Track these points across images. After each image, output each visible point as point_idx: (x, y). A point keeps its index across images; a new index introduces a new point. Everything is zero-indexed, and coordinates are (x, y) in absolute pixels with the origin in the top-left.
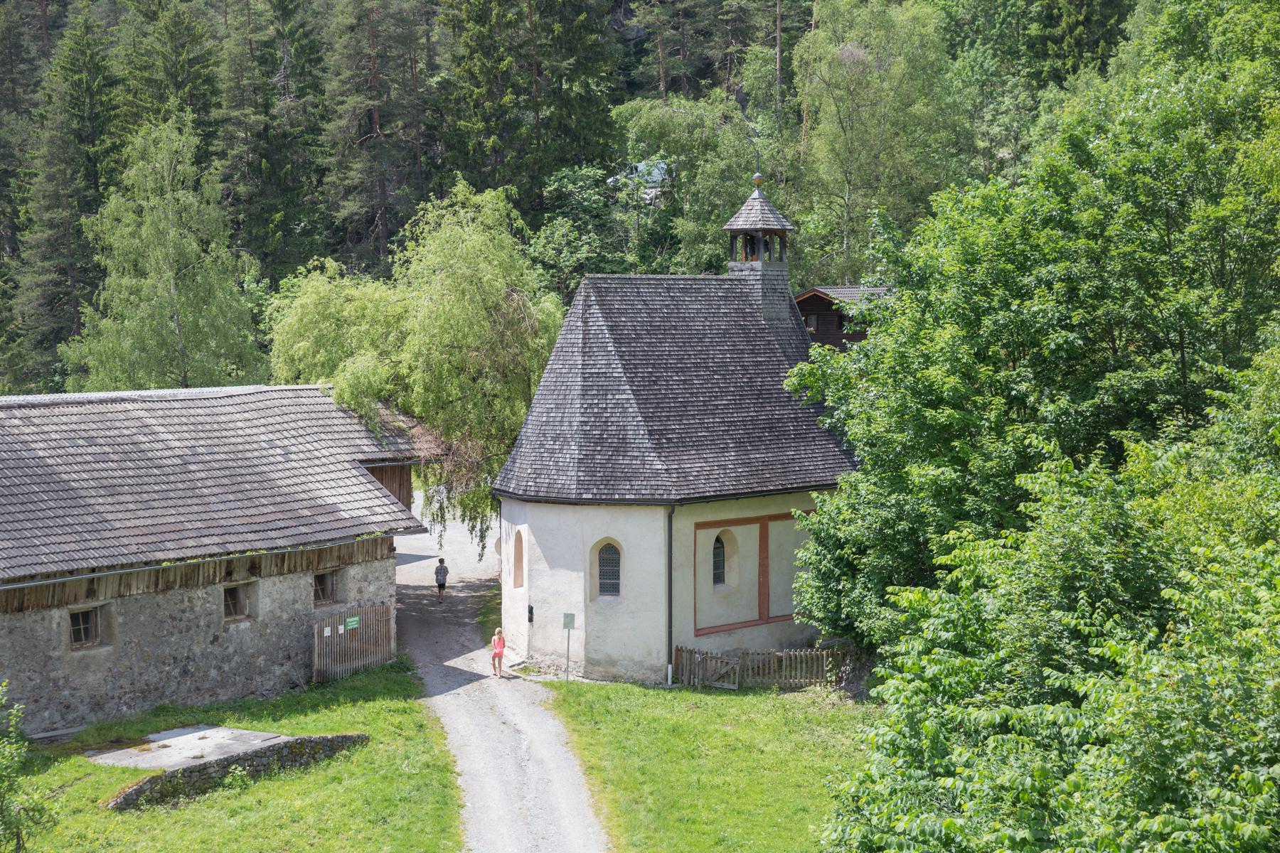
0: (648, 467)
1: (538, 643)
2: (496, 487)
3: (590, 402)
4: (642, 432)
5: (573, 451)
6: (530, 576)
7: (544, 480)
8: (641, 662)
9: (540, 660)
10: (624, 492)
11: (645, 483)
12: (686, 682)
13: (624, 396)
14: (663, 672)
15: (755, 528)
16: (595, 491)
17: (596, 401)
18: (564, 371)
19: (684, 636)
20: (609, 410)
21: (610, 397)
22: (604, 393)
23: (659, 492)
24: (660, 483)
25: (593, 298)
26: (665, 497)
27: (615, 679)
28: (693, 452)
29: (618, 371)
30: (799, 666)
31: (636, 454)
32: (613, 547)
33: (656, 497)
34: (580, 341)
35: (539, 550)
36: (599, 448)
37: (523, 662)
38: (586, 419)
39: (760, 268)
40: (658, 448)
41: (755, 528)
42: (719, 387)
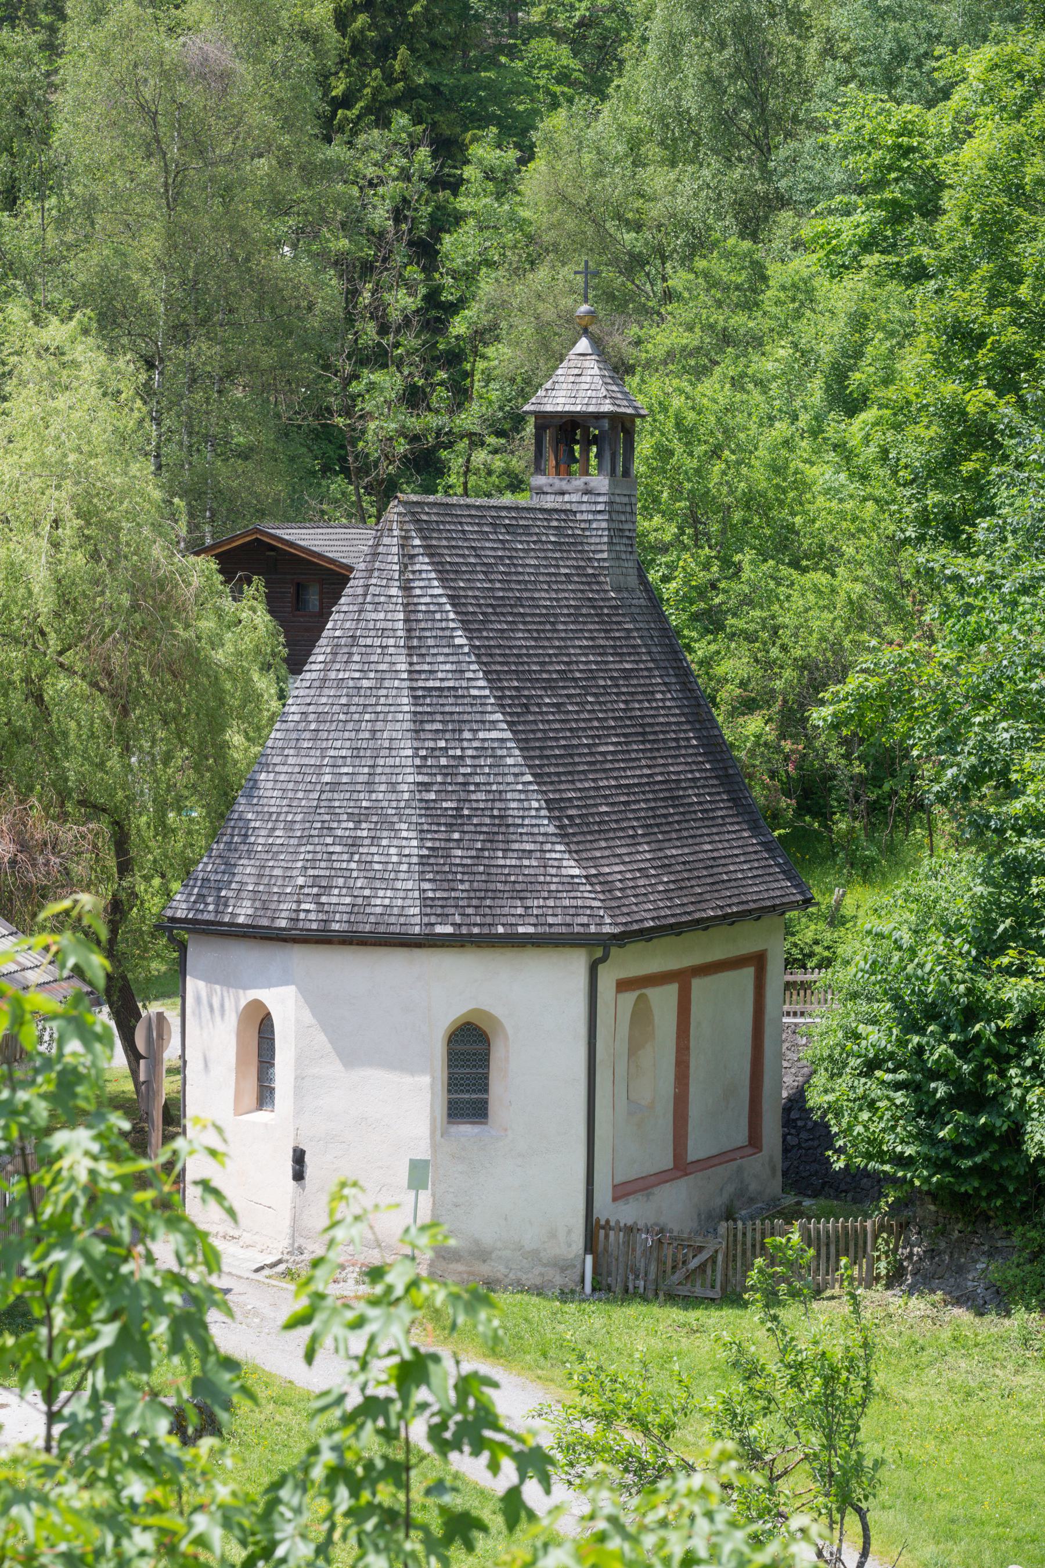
0: (553, 871)
2: (179, 914)
3: (431, 744)
4: (535, 804)
7: (338, 899)
8: (535, 1253)
10: (513, 920)
11: (551, 903)
12: (618, 1289)
13: (494, 735)
15: (672, 991)
16: (458, 919)
17: (442, 744)
18: (365, 683)
20: (469, 762)
21: (467, 735)
22: (455, 727)
24: (580, 903)
25: (417, 542)
26: (593, 929)
28: (603, 844)
29: (480, 687)
34: (400, 625)
35: (322, 1038)
36: (456, 836)
39: (605, 489)
40: (563, 836)
41: (672, 991)
42: (598, 719)
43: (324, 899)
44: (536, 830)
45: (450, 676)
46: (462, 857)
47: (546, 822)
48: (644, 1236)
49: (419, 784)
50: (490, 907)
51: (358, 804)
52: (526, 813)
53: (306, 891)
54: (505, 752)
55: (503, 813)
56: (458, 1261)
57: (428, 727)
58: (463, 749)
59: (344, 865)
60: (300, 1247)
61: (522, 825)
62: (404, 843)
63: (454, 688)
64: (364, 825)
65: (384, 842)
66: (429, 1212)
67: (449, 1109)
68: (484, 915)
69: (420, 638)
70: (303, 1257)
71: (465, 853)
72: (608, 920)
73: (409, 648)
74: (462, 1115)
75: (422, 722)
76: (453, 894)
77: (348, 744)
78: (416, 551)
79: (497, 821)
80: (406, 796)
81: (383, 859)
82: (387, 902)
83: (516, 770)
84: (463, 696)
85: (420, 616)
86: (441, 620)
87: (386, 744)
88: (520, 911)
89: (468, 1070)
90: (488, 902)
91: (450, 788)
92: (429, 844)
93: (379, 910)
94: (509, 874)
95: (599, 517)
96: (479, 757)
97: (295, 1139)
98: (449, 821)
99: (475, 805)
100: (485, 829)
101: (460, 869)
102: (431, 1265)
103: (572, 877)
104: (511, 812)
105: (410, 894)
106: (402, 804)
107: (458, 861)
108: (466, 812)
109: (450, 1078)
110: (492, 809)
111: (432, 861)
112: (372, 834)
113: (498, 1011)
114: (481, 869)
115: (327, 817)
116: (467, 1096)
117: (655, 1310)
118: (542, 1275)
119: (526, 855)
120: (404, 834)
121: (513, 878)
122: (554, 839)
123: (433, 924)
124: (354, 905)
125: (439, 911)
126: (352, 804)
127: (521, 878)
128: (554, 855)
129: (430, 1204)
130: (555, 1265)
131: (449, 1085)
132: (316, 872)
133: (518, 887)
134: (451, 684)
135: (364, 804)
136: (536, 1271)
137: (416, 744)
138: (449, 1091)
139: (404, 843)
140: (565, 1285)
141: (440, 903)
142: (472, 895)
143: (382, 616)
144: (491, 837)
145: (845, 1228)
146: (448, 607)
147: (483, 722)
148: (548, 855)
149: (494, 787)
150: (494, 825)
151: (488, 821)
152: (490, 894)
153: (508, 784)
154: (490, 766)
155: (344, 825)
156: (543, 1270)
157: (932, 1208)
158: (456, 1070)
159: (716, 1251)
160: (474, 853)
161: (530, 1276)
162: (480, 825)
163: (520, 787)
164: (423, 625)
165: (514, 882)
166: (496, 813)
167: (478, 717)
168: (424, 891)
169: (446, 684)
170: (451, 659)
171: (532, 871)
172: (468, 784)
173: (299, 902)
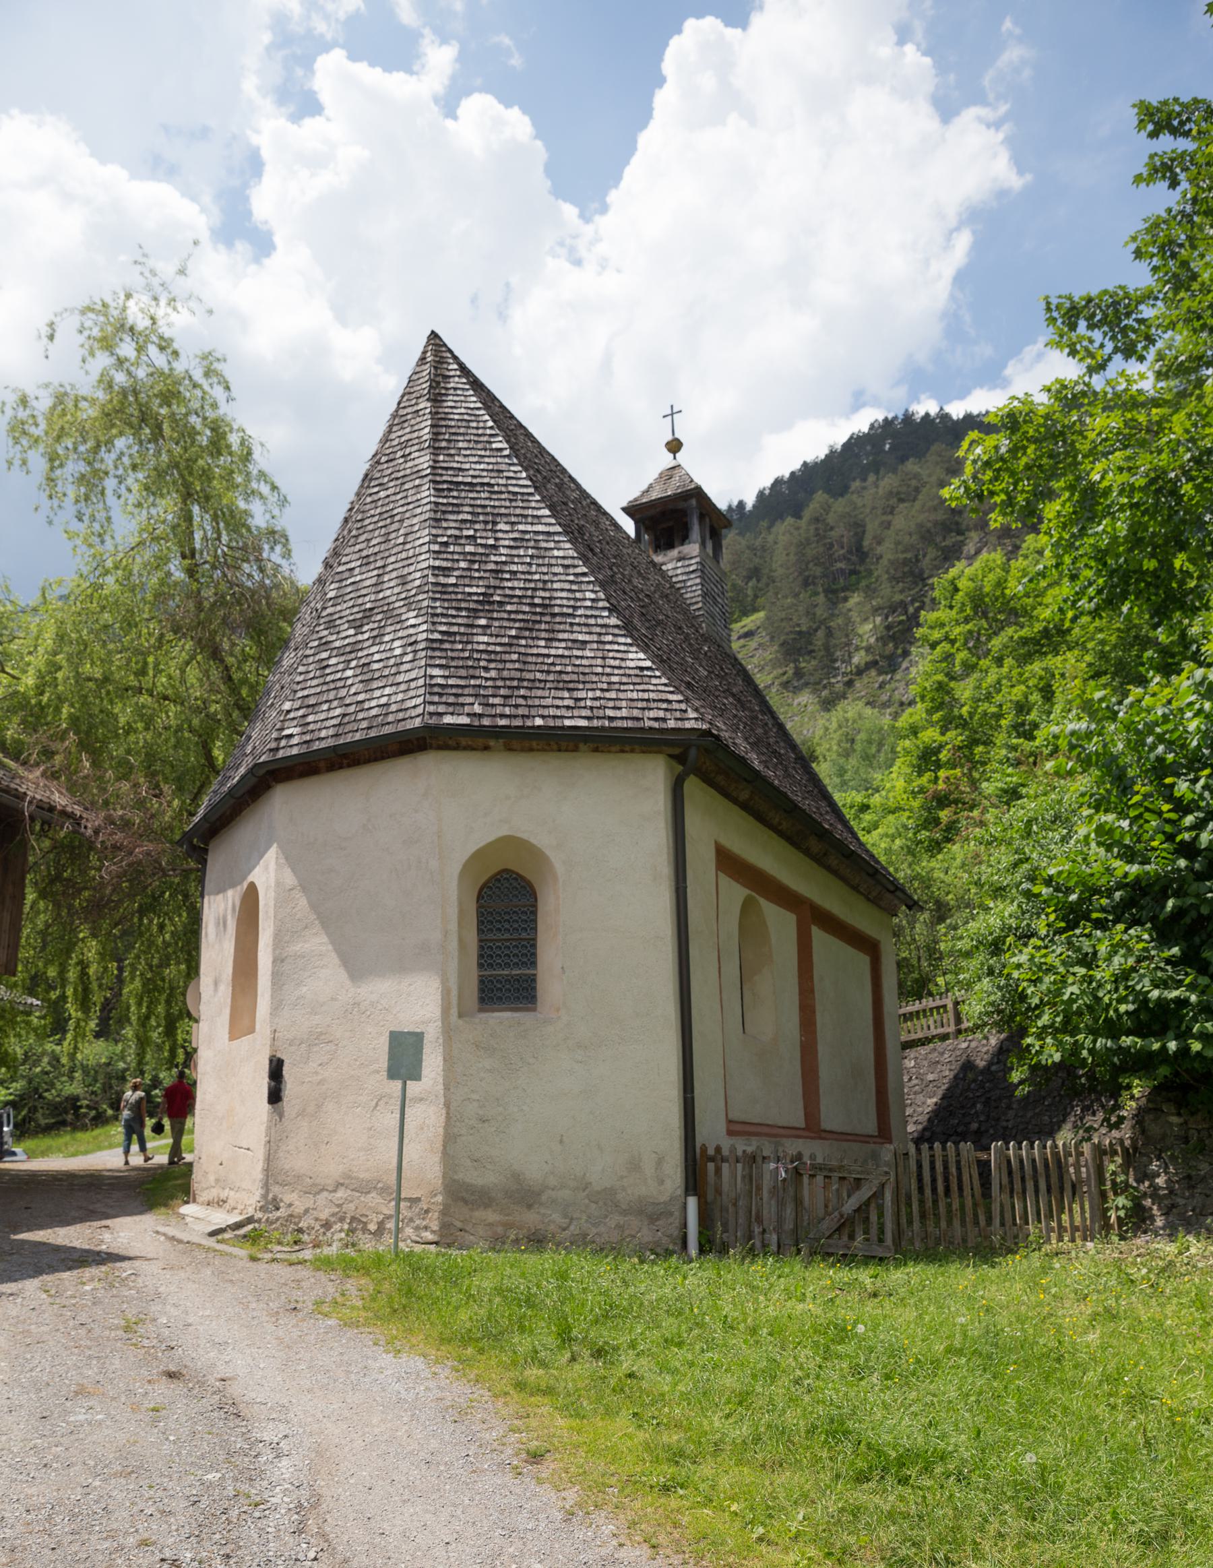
1: (296, 1161)
5: (417, 625)
6: (276, 976)
8: (610, 1192)
9: (299, 1208)
11: (613, 695)
16: (477, 709)
20: (503, 551)
23: (652, 714)
24: (652, 696)
26: (671, 724)
27: (537, 1241)
30: (1030, 1185)
31: (581, 637)
32: (519, 877)
33: (648, 724)
35: (303, 902)
37: (250, 1220)
38: (444, 564)
43: (310, 718)
44: (592, 621)
45: (485, 474)
46: (488, 644)
47: (606, 614)
48: (772, 1166)
49: (434, 568)
50: (524, 697)
51: (363, 608)
52: (579, 604)
53: (292, 715)
54: (552, 545)
55: (547, 602)
56: (487, 1206)
58: (496, 539)
59: (339, 675)
60: (274, 1199)
61: (574, 616)
62: (412, 631)
63: (488, 484)
64: (365, 628)
65: (387, 638)
66: (441, 1131)
67: (481, 990)
68: (516, 706)
69: (449, 441)
70: (278, 1214)
71: (493, 640)
73: (435, 448)
75: (444, 512)
76: (472, 682)
77: (357, 556)
78: (452, 373)
79: (538, 610)
80: (417, 583)
81: (383, 656)
82: (384, 700)
83: (566, 562)
84: (501, 493)
85: (453, 423)
86: (477, 428)
87: (401, 540)
88: (571, 703)
89: (507, 936)
90: (522, 692)
91: (477, 575)
92: (444, 628)
93: (374, 712)
94: (553, 664)
95: (692, 576)
97: (272, 1045)
98: (472, 605)
99: (508, 592)
100: (520, 617)
101: (484, 656)
102: (445, 1212)
103: (642, 669)
104: (558, 602)
105: (413, 685)
106: (413, 592)
107: (482, 647)
108: (497, 598)
109: (481, 948)
110: (532, 597)
112: (375, 633)
113: (541, 840)
114: (515, 657)
115: (326, 633)
116: (505, 972)
118: (619, 1227)
119: (578, 645)
120: (412, 622)
121: (558, 668)
122: (616, 631)
123: (441, 714)
124: (344, 715)
125: (451, 700)
126: (356, 609)
127: (569, 669)
128: (616, 647)
129: (442, 1119)
130: (640, 1212)
131: (481, 956)
132: (306, 693)
133: (566, 677)
134: (486, 480)
135: (368, 606)
136: (612, 1222)
137: (434, 531)
138: (480, 966)
139: (412, 631)
141: (454, 691)
142: (500, 683)
143: (408, 430)
144: (530, 625)
146: (487, 417)
147: (526, 516)
148: (608, 647)
149: (537, 577)
150: (535, 613)
151: (527, 609)
152: (525, 684)
153: (555, 574)
154: (532, 557)
155: (343, 634)
156: (621, 1220)
158: (490, 936)
159: (883, 1185)
160: (506, 640)
161: (602, 1229)
162: (517, 612)
163: (571, 578)
164: (453, 430)
165: (560, 672)
166: (537, 601)
167: (518, 511)
168: (432, 677)
169: (479, 480)
170: (487, 460)
171: (585, 662)
172: (503, 572)
173: (282, 729)
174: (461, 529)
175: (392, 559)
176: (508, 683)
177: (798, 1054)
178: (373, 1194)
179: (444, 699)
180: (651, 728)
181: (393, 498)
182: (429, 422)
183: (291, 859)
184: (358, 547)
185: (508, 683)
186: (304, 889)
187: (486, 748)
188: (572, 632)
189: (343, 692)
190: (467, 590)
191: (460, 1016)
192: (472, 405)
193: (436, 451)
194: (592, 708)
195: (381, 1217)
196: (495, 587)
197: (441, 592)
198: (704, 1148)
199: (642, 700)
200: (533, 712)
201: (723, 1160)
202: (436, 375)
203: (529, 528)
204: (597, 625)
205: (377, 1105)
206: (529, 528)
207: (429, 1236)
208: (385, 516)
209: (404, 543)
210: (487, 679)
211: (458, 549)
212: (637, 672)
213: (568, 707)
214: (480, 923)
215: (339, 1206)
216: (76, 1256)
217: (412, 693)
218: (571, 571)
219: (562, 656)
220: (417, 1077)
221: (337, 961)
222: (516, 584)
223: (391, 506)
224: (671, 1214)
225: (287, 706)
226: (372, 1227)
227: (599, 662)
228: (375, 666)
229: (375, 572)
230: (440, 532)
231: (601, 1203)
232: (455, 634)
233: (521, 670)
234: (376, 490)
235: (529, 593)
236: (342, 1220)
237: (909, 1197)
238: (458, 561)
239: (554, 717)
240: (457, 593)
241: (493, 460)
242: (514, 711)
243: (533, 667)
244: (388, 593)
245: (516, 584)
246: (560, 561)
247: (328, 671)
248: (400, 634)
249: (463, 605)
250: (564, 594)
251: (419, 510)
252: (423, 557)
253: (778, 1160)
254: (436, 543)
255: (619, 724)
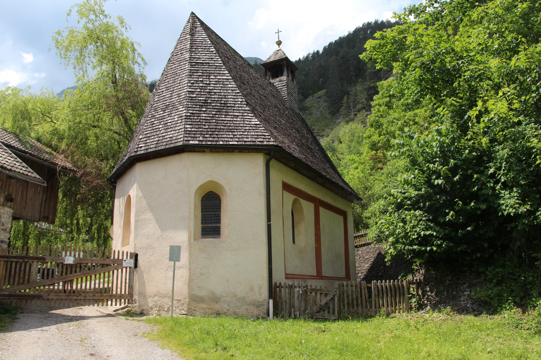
4: (240, 100)
11: (246, 133)
14: (265, 307)
16: (201, 139)
19: (279, 277)
20: (212, 85)
23: (259, 140)
24: (259, 134)
26: (265, 143)
27: (218, 314)
30: (385, 295)
31: (236, 114)
33: (258, 143)
35: (145, 202)
38: (192, 90)
44: (240, 109)
45: (207, 59)
46: (205, 117)
48: (298, 289)
49: (189, 91)
50: (217, 135)
51: (166, 104)
53: (142, 140)
54: (228, 83)
56: (203, 302)
57: (195, 74)
58: (210, 81)
59: (157, 127)
61: (234, 107)
62: (181, 113)
63: (208, 63)
65: (173, 115)
66: (188, 278)
67: (202, 231)
68: (214, 138)
69: (196, 49)
70: (136, 305)
71: (207, 115)
72: (272, 140)
73: (191, 51)
74: (208, 234)
75: (193, 73)
76: (200, 130)
77: (165, 87)
78: (198, 26)
79: (223, 105)
80: (183, 96)
82: (171, 136)
83: (233, 89)
84: (212, 66)
86: (205, 44)
87: (179, 82)
88: (232, 136)
89: (211, 213)
90: (216, 133)
91: (203, 93)
92: (191, 112)
93: (168, 140)
94: (227, 123)
96: (217, 84)
97: (135, 249)
98: (201, 104)
99: (213, 99)
100: (217, 107)
102: (189, 304)
103: (256, 124)
104: (230, 102)
105: (180, 131)
106: (182, 100)
107: (203, 118)
108: (209, 101)
109: (202, 217)
111: (192, 118)
112: (169, 113)
113: (222, 181)
114: (214, 121)
115: (154, 112)
117: (302, 322)
119: (236, 117)
120: (181, 109)
121: (228, 125)
122: (248, 112)
123: (189, 141)
125: (193, 136)
126: (163, 105)
127: (232, 125)
128: (248, 117)
129: (188, 274)
131: (202, 220)
132: (147, 132)
133: (231, 128)
135: (167, 104)
136: (244, 307)
138: (202, 223)
139: (181, 113)
140: (259, 315)
141: (194, 133)
142: (209, 130)
143: (183, 45)
144: (220, 110)
145: (394, 285)
146: (209, 41)
148: (245, 117)
149: (223, 94)
150: (222, 106)
151: (219, 105)
152: (217, 130)
154: (221, 87)
157: (433, 272)
158: (206, 213)
159: (334, 295)
160: (211, 115)
161: (241, 310)
162: (216, 106)
163: (234, 94)
164: (197, 45)
165: (229, 126)
166: (222, 102)
167: (217, 72)
168: (187, 128)
169: (205, 62)
170: (208, 55)
171: (237, 122)
174: (198, 78)
175: (176, 88)
176: (212, 130)
177: (314, 251)
178: (166, 298)
179: (190, 136)
180: (258, 145)
181: (177, 68)
182: (189, 43)
183: (141, 188)
184: (165, 84)
185: (212, 130)
186: (145, 198)
187: (204, 152)
188: (234, 112)
189: (158, 133)
190: (199, 99)
191: (194, 240)
192: (204, 37)
193: (191, 52)
194: (239, 138)
195: (169, 306)
196: (209, 98)
197: (191, 100)
198: (276, 284)
199: (256, 135)
200: (220, 139)
201: (282, 287)
202: (193, 27)
203: (221, 77)
204: (242, 110)
205: (167, 269)
206: (221, 77)
207: (184, 312)
208: (174, 73)
209: (180, 83)
210: (205, 128)
211: (197, 85)
212: (255, 126)
213: (231, 138)
214: (202, 209)
215: (155, 302)
216: (69, 318)
217: (180, 133)
218: (234, 92)
219: (230, 121)
220: (179, 261)
221: (155, 222)
222: (216, 96)
223: (176, 70)
224: (264, 305)
225: (141, 137)
226: (166, 309)
227: (242, 122)
228: (169, 124)
229: (170, 93)
230: (191, 79)
231: (241, 302)
232: (195, 113)
233: (216, 126)
234: (172, 65)
235: (220, 99)
236: (156, 307)
237: (344, 299)
238: (197, 89)
239: (226, 141)
240: (196, 100)
241: (210, 55)
242: (213, 139)
243: (220, 124)
244: (174, 99)
245: (216, 96)
246: (231, 89)
247: (154, 125)
248: (177, 113)
249: (198, 104)
250: (232, 100)
251: (185, 72)
252: (186, 88)
253: (300, 287)
254: (190, 83)
255: (248, 143)
